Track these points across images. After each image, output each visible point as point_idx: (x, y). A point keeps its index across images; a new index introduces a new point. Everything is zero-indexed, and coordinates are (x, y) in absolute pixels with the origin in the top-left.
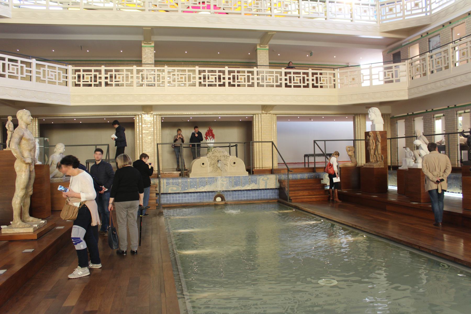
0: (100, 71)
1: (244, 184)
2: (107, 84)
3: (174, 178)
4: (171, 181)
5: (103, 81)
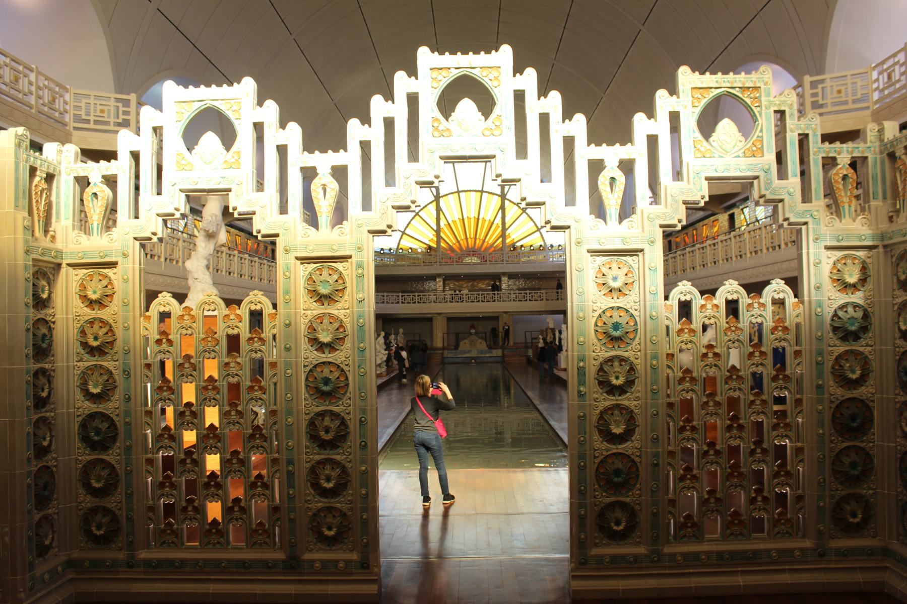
0: (415, 296)
1: (486, 353)
2: (418, 302)
3: (452, 350)
4: (449, 351)
5: (417, 301)
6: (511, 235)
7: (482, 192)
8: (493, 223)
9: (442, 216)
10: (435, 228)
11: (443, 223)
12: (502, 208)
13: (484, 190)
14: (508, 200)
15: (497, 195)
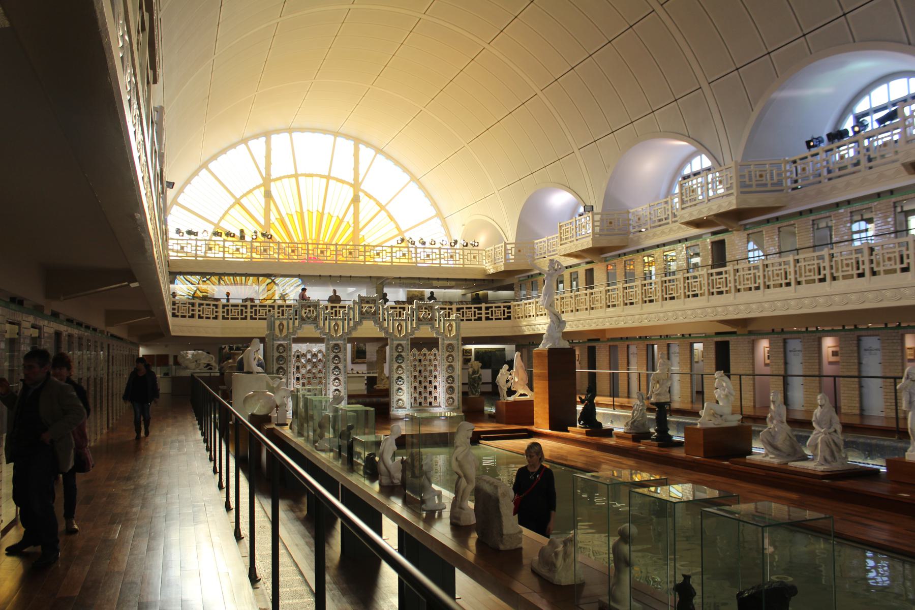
6: (365, 237)
7: (328, 178)
8: (341, 221)
9: (272, 206)
10: (262, 222)
11: (274, 216)
12: (356, 200)
13: (332, 175)
14: (363, 191)
15: (348, 183)
